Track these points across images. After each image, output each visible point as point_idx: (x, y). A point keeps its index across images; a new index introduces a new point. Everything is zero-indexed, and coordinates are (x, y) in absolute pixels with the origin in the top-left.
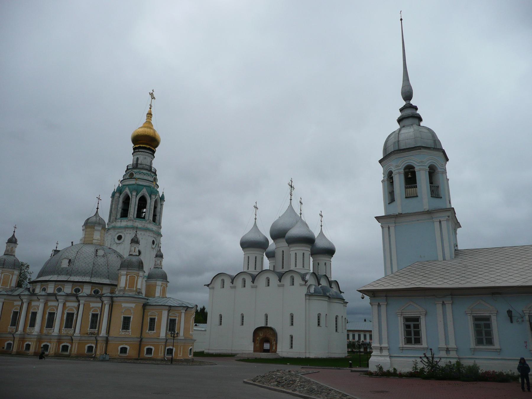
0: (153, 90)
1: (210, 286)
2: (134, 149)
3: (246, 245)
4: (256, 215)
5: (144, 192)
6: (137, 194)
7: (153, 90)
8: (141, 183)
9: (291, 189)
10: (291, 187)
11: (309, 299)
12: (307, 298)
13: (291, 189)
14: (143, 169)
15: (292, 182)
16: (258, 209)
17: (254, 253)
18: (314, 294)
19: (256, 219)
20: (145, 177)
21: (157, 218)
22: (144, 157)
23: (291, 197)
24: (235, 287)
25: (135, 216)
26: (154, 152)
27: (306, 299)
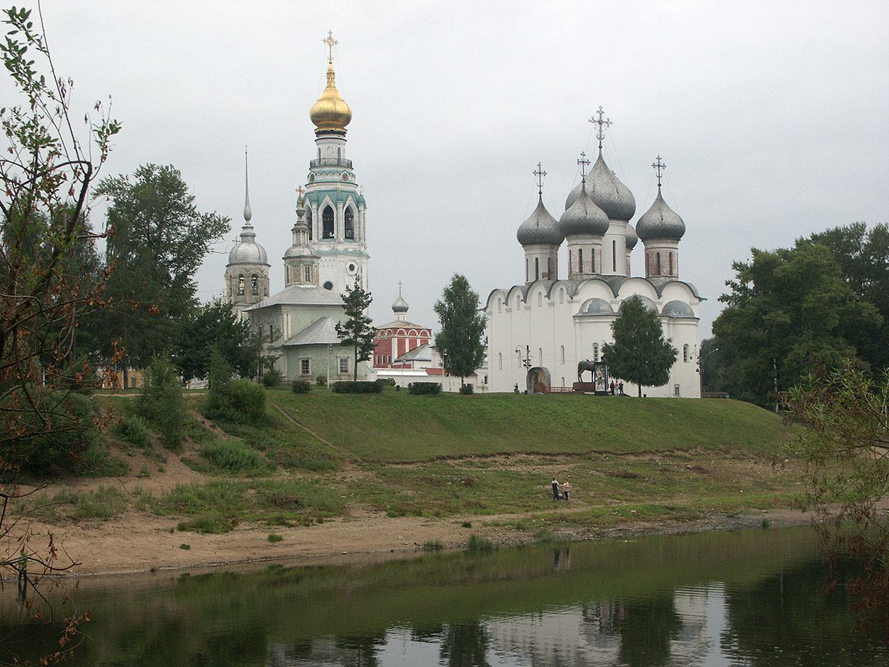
0: (330, 33)
1: (487, 311)
2: (318, 134)
3: (527, 239)
4: (540, 187)
5: (327, 200)
6: (318, 206)
7: (330, 33)
8: (323, 188)
9: (601, 128)
10: (600, 123)
11: (581, 323)
12: (577, 321)
13: (601, 128)
14: (325, 165)
15: (601, 113)
16: (545, 174)
17: (538, 252)
18: (587, 315)
19: (540, 193)
20: (329, 178)
21: (356, 232)
22: (327, 146)
23: (600, 142)
24: (509, 311)
25: (321, 237)
26: (344, 134)
27: (575, 323)
